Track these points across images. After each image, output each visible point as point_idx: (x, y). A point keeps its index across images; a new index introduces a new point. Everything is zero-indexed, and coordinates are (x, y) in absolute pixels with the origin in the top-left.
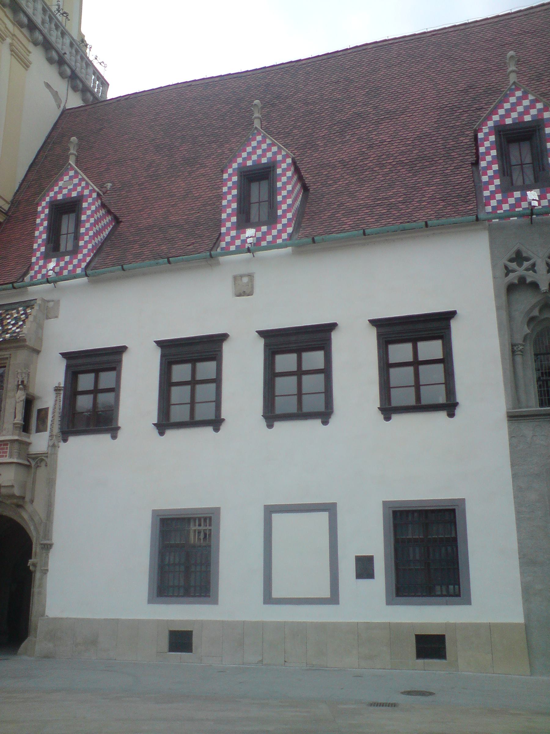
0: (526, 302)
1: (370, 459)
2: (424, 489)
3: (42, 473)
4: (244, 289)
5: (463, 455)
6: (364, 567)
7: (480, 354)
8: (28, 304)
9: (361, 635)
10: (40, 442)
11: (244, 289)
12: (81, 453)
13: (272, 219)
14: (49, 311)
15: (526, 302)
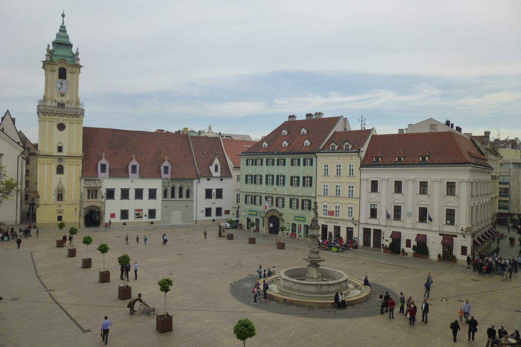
0: (164, 187)
1: (146, 204)
2: (152, 208)
3: (103, 204)
4: (132, 182)
5: (157, 204)
6: (146, 216)
7: (159, 194)
8: (99, 180)
9: (145, 222)
10: (103, 200)
11: (132, 182)
12: (109, 202)
13: (136, 173)
14: (103, 182)
15: (164, 187)
